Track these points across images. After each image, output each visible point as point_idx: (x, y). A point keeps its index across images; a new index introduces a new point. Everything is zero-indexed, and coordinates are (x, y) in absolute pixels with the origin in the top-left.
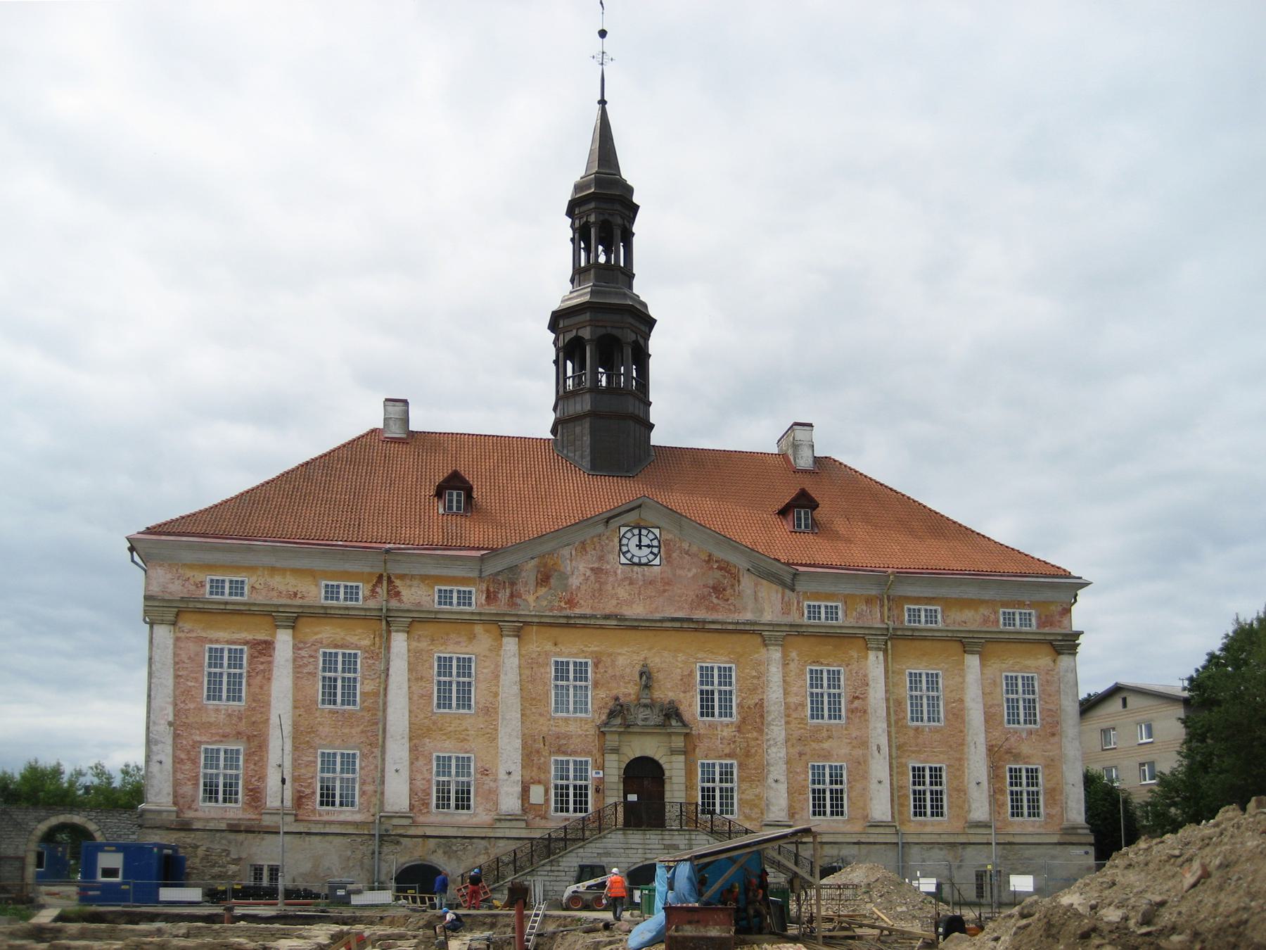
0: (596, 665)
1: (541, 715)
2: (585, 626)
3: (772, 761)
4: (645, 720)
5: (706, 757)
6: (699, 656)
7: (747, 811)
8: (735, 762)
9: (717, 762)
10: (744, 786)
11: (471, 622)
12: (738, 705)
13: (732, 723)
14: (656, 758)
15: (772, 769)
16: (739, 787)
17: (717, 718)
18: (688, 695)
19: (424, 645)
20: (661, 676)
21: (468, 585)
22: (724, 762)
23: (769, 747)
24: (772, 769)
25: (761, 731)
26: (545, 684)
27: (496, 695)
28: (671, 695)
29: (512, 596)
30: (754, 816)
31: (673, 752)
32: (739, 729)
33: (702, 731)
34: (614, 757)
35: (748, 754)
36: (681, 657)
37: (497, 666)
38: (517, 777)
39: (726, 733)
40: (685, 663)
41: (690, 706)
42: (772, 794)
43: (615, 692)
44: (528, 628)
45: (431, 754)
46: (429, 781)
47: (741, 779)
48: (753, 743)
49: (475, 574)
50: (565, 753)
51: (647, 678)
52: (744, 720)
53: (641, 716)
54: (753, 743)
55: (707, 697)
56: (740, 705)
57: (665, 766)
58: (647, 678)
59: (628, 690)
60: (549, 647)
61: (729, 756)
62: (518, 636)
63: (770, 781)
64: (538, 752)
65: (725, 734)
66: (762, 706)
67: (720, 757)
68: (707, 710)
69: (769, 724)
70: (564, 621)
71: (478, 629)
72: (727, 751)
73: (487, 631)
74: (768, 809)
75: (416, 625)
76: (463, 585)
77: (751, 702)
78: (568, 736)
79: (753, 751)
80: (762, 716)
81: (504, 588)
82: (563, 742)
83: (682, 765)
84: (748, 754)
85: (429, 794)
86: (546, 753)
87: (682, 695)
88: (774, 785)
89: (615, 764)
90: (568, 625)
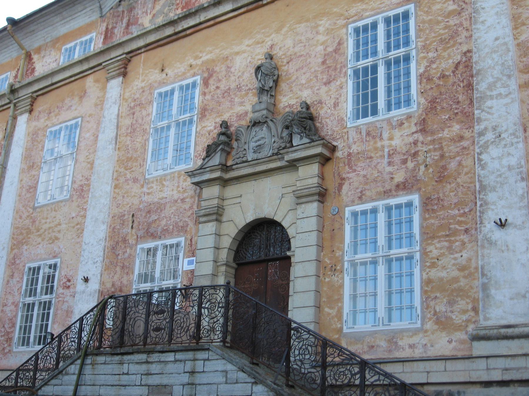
0: (206, 82)
1: (135, 180)
2: (197, 28)
3: (491, 180)
4: (259, 148)
5: (361, 199)
6: (353, 11)
7: (441, 307)
8: (415, 198)
9: (380, 204)
10: (435, 249)
11: (82, 75)
12: (421, 77)
13: (409, 117)
14: (278, 219)
15: (491, 197)
16: (424, 253)
17: (382, 115)
18: (333, 86)
19: (41, 123)
20: (292, 68)
21: (90, 32)
22: (393, 202)
23: (485, 147)
24: (491, 197)
25: (468, 119)
26: (144, 131)
27: (92, 164)
28: (307, 95)
29: (128, 25)
30: (458, 318)
31: (301, 198)
32: (423, 127)
33: (355, 148)
34: (210, 227)
35: (442, 176)
36: (324, 24)
37: (99, 123)
38: (94, 285)
39: (399, 140)
40: (328, 31)
41: (336, 105)
42: (492, 258)
43: (225, 117)
44: (135, 60)
45: (24, 266)
46: (17, 306)
47: (428, 235)
48: (453, 149)
49: (95, 16)
50: (154, 236)
51: (269, 77)
52: (432, 106)
53: (253, 145)
54: (452, 149)
55: (366, 80)
56: (425, 78)
57: (291, 232)
58: (269, 77)
59: (242, 107)
60: (155, 76)
61: (404, 187)
62: (124, 75)
63: (489, 226)
64: (125, 240)
65: (397, 142)
66: (468, 66)
67: (387, 194)
68: (366, 105)
69: (483, 99)
70: (169, 31)
71: (90, 81)
72: (399, 177)
73: (97, 81)
74: (488, 296)
75: (40, 99)
76: (81, 36)
77: (447, 65)
78: (160, 207)
79: (453, 165)
80: (470, 86)
81: (122, 20)
82: (154, 217)
83: (312, 223)
84: (442, 176)
85: (14, 325)
86: (132, 241)
87: (324, 89)
88: (498, 234)
89: (210, 241)
90: (176, 37)
